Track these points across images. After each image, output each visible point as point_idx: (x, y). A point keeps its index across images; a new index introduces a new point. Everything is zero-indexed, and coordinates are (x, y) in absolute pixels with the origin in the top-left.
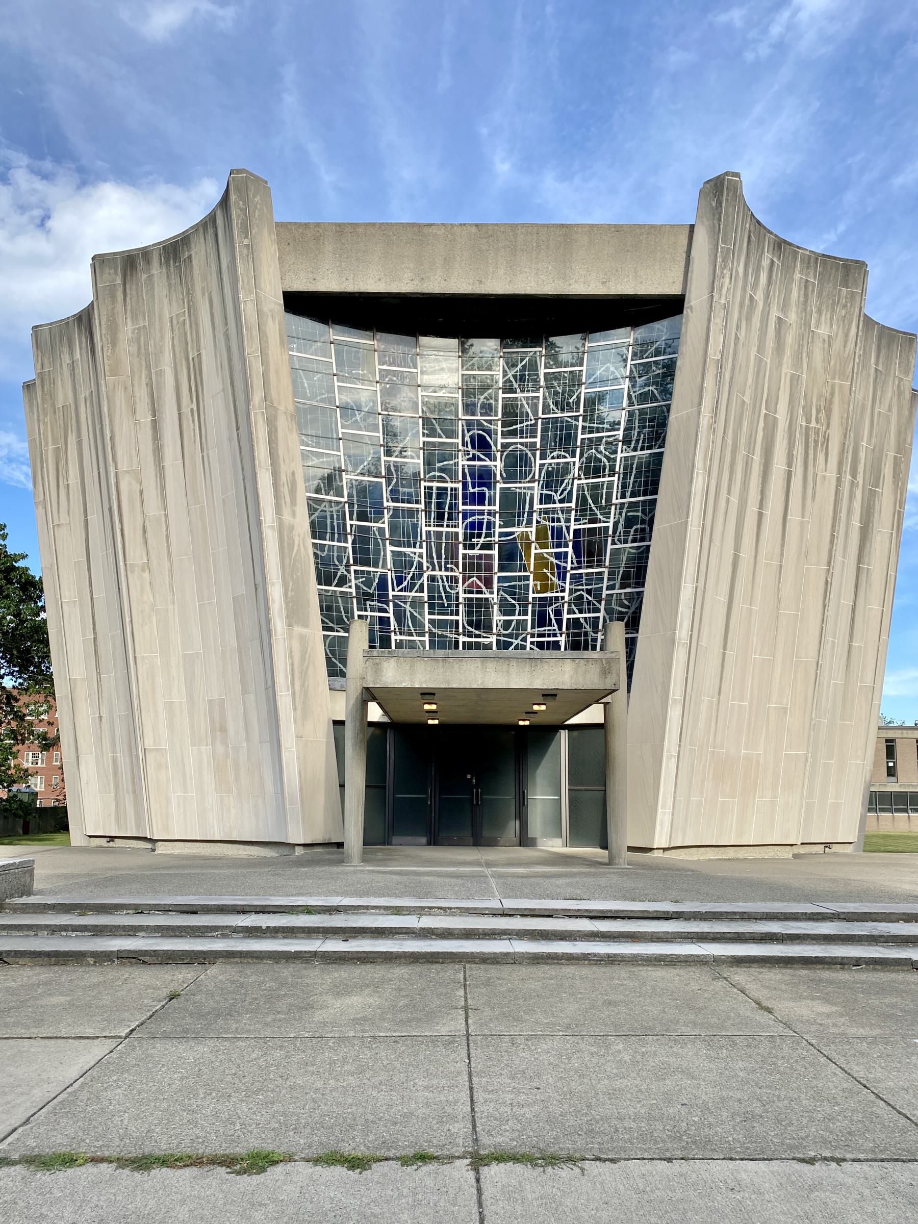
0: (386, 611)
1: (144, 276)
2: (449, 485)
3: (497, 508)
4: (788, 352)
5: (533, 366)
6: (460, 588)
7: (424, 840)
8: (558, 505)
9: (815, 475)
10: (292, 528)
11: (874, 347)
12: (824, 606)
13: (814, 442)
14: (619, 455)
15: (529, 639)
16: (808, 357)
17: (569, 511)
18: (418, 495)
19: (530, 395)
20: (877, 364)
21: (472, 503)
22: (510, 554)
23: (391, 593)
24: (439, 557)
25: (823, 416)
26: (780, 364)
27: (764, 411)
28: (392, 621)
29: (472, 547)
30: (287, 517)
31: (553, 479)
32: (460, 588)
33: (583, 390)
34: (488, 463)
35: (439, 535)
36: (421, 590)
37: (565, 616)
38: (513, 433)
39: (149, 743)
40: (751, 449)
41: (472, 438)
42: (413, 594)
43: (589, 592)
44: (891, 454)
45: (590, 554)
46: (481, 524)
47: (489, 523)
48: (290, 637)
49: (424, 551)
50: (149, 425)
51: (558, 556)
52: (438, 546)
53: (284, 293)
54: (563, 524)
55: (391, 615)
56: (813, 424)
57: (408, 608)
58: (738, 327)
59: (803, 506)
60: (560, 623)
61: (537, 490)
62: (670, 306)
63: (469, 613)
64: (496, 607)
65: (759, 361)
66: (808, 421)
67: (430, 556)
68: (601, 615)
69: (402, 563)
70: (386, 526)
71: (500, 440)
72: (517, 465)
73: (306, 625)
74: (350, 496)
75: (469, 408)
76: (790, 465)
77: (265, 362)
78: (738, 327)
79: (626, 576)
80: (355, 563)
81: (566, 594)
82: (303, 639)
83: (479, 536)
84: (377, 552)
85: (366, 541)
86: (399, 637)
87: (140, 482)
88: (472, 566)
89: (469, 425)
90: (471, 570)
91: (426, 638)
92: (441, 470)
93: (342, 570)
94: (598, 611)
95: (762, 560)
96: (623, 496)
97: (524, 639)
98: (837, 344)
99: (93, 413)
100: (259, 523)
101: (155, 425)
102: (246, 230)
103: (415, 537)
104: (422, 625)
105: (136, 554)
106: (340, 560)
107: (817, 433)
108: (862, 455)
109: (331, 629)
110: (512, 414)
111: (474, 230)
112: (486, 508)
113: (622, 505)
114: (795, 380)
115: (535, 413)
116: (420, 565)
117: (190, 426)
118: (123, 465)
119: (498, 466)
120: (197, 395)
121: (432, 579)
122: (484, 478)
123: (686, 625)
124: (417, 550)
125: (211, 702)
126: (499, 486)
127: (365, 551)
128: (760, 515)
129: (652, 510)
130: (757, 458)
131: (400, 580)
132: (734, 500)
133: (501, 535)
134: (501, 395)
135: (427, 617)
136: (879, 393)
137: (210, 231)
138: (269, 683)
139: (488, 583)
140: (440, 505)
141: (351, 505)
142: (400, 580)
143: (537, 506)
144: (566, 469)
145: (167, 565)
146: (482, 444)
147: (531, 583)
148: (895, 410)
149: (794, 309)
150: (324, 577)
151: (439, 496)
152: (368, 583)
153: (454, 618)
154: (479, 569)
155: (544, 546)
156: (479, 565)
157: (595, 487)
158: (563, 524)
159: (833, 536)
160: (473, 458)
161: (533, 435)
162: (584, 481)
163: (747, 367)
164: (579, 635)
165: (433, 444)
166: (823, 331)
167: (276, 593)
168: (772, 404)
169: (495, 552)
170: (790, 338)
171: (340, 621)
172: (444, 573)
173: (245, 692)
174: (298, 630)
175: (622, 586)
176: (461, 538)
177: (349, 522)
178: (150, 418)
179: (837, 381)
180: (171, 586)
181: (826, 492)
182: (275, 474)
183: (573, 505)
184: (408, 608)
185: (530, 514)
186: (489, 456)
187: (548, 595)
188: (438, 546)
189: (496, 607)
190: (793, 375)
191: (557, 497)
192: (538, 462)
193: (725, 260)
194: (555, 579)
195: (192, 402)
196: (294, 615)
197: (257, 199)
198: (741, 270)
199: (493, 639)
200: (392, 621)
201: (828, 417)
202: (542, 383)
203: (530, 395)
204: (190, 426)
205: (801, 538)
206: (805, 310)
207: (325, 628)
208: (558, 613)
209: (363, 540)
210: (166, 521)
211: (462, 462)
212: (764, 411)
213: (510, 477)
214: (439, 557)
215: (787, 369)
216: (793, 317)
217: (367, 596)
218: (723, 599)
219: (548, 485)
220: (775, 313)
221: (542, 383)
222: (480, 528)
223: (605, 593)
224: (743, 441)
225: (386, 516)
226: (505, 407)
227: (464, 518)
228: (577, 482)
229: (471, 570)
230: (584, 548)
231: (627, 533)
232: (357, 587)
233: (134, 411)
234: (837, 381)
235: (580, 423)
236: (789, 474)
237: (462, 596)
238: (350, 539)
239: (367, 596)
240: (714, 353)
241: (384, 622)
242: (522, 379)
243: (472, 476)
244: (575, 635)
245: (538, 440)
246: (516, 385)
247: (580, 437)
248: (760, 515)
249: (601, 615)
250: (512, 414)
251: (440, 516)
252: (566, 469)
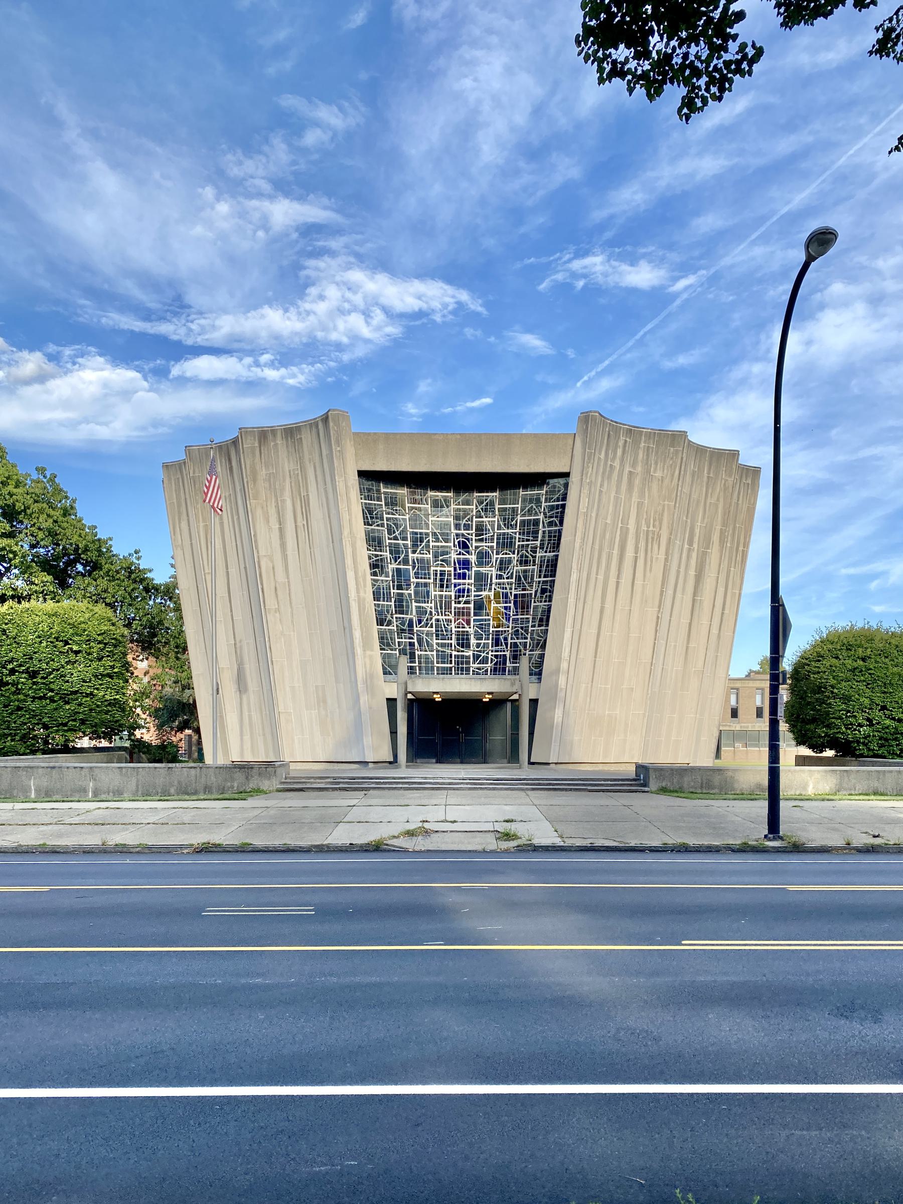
0: (412, 638)
2: (447, 569)
3: (472, 581)
4: (636, 489)
5: (492, 503)
6: (453, 625)
7: (434, 761)
8: (506, 580)
9: (652, 557)
10: (364, 599)
11: (707, 463)
12: (656, 631)
13: (652, 538)
14: (538, 555)
15: (490, 653)
16: (648, 490)
17: (511, 584)
18: (429, 574)
19: (491, 519)
20: (709, 473)
21: (459, 578)
22: (480, 606)
23: (415, 629)
24: (441, 608)
25: (657, 523)
26: (631, 497)
27: (620, 525)
28: (416, 644)
29: (459, 602)
30: (362, 594)
31: (503, 565)
32: (453, 625)
33: (519, 518)
34: (467, 556)
35: (441, 596)
36: (432, 627)
37: (509, 641)
38: (481, 540)
39: (281, 709)
40: (611, 547)
41: (459, 542)
42: (427, 629)
43: (522, 628)
44: (719, 527)
45: (523, 608)
46: (464, 590)
47: (468, 589)
48: (365, 657)
49: (433, 605)
50: (277, 530)
51: (506, 608)
52: (441, 602)
53: (359, 471)
54: (508, 591)
55: (415, 641)
56: (651, 528)
57: (424, 636)
58: (601, 486)
59: (645, 576)
60: (506, 644)
61: (494, 572)
62: (566, 475)
63: (458, 639)
64: (472, 636)
65: (617, 499)
66: (648, 527)
67: (436, 608)
68: (528, 641)
69: (421, 612)
70: (412, 592)
71: (474, 544)
72: (483, 558)
73: (372, 650)
74: (393, 576)
75: (457, 527)
76: (636, 553)
77: (350, 514)
78: (601, 486)
79: (541, 620)
80: (396, 613)
81: (510, 629)
82: (371, 657)
83: (463, 596)
84: (408, 607)
85: (401, 601)
86: (420, 653)
87: (272, 562)
88: (459, 613)
89: (457, 535)
90: (459, 615)
91: (435, 653)
92: (442, 560)
93: (389, 617)
94: (526, 638)
95: (619, 607)
96: (540, 577)
97: (488, 653)
98: (667, 481)
99: (231, 509)
100: (348, 598)
101: (281, 530)
102: (338, 443)
103: (428, 598)
104: (432, 646)
105: (271, 602)
106: (388, 612)
107: (653, 533)
108: (697, 531)
109: (384, 649)
110: (480, 529)
111: (458, 437)
112: (467, 581)
113: (539, 582)
114: (640, 505)
115: (493, 530)
116: (431, 612)
117: (302, 534)
118: (262, 552)
119: (473, 558)
120: (307, 515)
121: (438, 620)
122: (466, 564)
123: (568, 650)
124: (429, 605)
125: (317, 687)
126: (474, 569)
127: (401, 607)
128: (618, 583)
129: (552, 586)
130: (616, 552)
131: (420, 621)
132: (601, 577)
133: (475, 596)
134: (475, 519)
135: (435, 641)
136: (710, 491)
137: (314, 429)
138: (353, 679)
139: (468, 623)
140: (441, 580)
141: (393, 582)
142: (420, 621)
143: (494, 581)
144: (510, 561)
145: (290, 610)
146: (464, 546)
147: (491, 622)
148: (721, 500)
149: (640, 464)
150: (380, 622)
151: (441, 575)
152: (403, 624)
153: (450, 641)
154: (463, 615)
155: (498, 603)
156: (463, 613)
157: (525, 571)
158: (508, 591)
159: (662, 592)
160: (460, 554)
161: (492, 540)
162: (519, 568)
163: (609, 503)
164: (516, 651)
165: (438, 547)
166: (659, 474)
167: (357, 634)
168: (625, 521)
169: (472, 606)
170: (637, 481)
171: (388, 645)
172: (444, 617)
173: (337, 681)
174: (368, 653)
175: (539, 626)
176: (453, 598)
177: (392, 591)
178: (278, 526)
179: (666, 503)
180: (292, 622)
181: (658, 568)
182: (356, 573)
183: (513, 580)
184: (424, 636)
185: (491, 585)
186: (468, 552)
187: (500, 629)
188: (441, 602)
189: (472, 636)
190: (639, 503)
192: (495, 556)
193: (589, 459)
194: (504, 621)
196: (366, 645)
197: (344, 424)
198: (602, 456)
199: (471, 653)
200: (416, 644)
201: (661, 524)
202: (497, 513)
203: (491, 519)
204: (302, 534)
205: (643, 593)
206: (647, 463)
207: (381, 649)
208: (506, 639)
209: (400, 600)
210: (289, 586)
211: (454, 556)
212: (620, 525)
213: (480, 564)
214: (441, 608)
215: (635, 499)
216: (639, 469)
217: (403, 631)
218: (594, 631)
219: (500, 569)
220: (627, 469)
221: (497, 513)
222: (464, 592)
223: (530, 629)
224: (606, 544)
225: (412, 587)
226: (477, 526)
227: (455, 586)
228: (516, 568)
229: (459, 615)
230: (519, 605)
231: (542, 597)
232: (397, 626)
233: (268, 522)
234: (666, 503)
235: (517, 536)
236: (636, 558)
237: (454, 630)
238: (393, 600)
239: (403, 631)
240: (583, 509)
241: (412, 645)
242: (486, 510)
243: (459, 564)
244: (515, 651)
245: (495, 544)
246: (483, 514)
247: (517, 543)
248: (618, 583)
249: (528, 641)
250: (480, 529)
251: (442, 586)
252: (510, 561)
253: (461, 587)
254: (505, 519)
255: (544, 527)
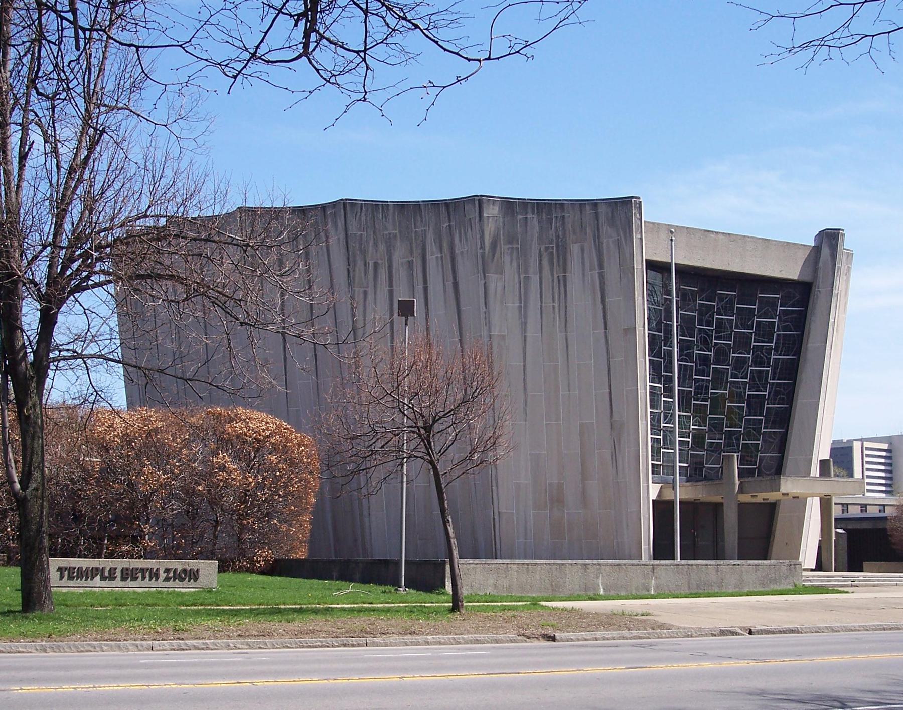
1: (520, 217)
5: (731, 302)
14: (773, 357)
43: (754, 429)
97: (720, 454)
169: (708, 403)
191: (740, 376)
195: (554, 301)
223: (763, 430)
237: (692, 427)
253: (701, 383)
254: (742, 319)
255: (778, 330)
